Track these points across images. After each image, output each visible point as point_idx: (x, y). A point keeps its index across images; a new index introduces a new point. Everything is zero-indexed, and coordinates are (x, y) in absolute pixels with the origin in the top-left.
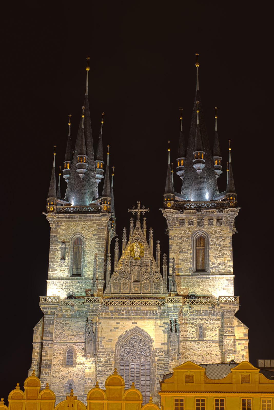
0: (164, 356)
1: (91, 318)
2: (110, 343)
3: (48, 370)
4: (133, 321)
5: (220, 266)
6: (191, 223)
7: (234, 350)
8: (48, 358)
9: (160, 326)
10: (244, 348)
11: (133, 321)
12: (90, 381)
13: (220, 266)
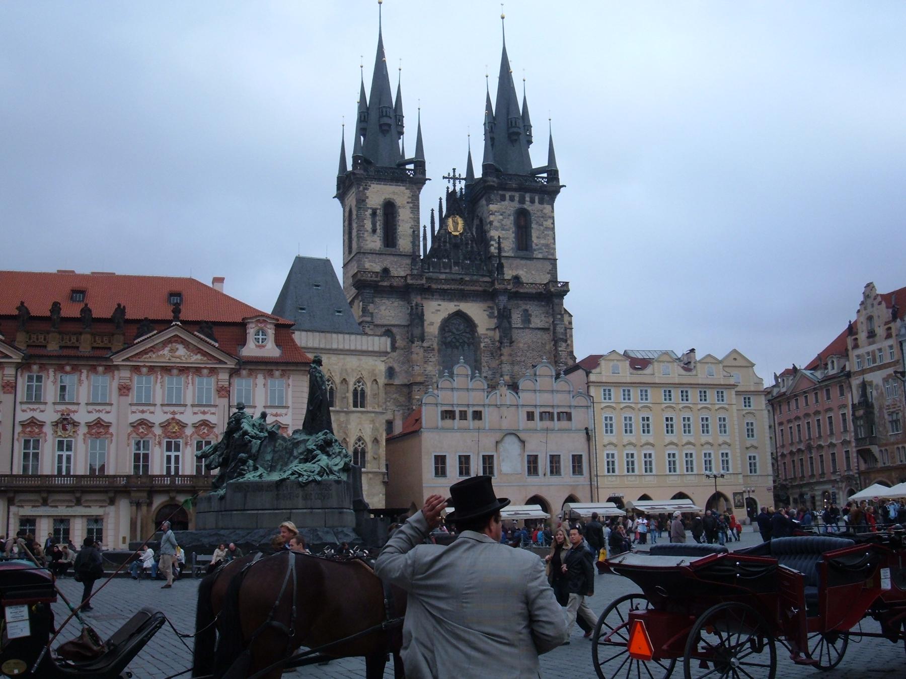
6: (512, 199)
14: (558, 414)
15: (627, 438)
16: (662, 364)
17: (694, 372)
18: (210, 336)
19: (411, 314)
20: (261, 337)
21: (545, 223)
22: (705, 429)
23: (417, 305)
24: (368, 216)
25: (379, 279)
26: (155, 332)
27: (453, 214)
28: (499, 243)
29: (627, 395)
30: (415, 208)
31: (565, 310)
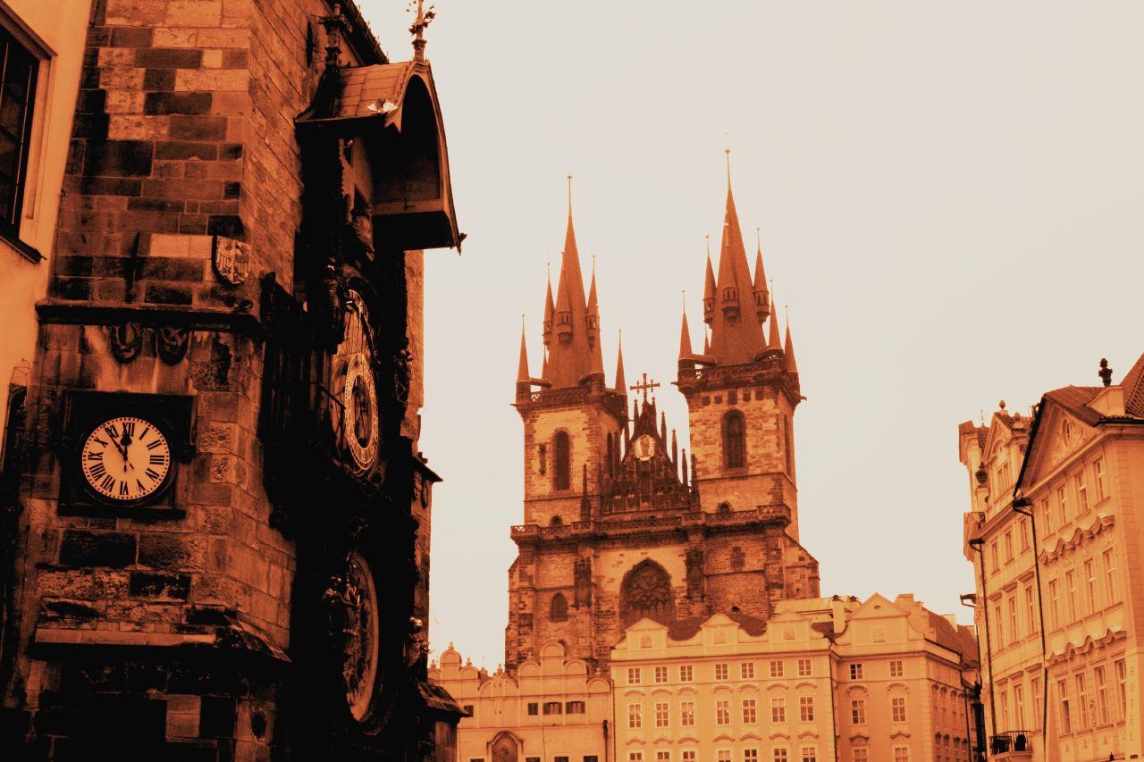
2: (612, 584)
3: (526, 628)
5: (763, 459)
6: (719, 400)
8: (528, 611)
9: (680, 556)
10: (798, 578)
11: (643, 551)
12: (582, 641)
14: (568, 704)
15: (660, 732)
16: (713, 629)
17: (763, 637)
19: (575, 574)
22: (778, 715)
23: (583, 561)
27: (642, 434)
29: (661, 675)
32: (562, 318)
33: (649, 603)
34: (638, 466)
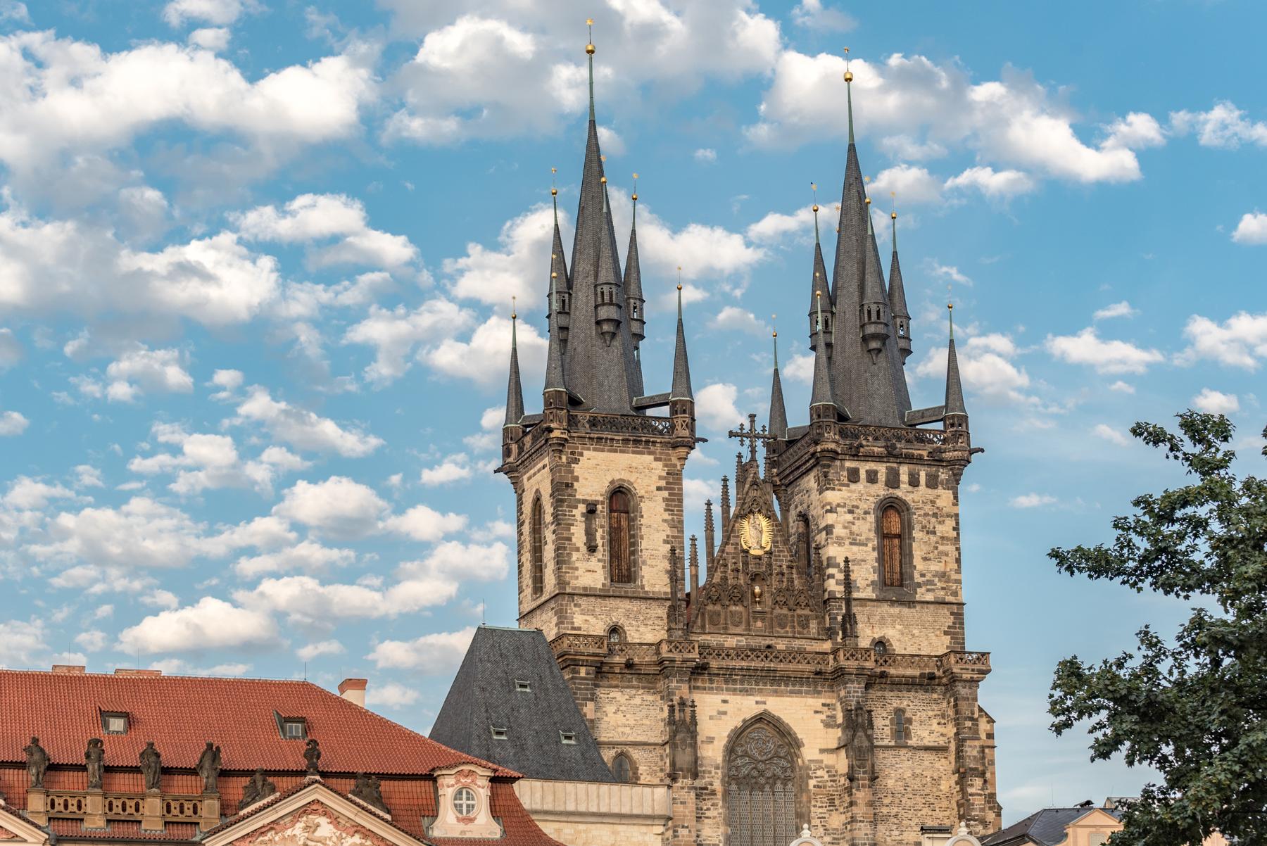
0: (826, 777)
1: (677, 688)
2: (710, 746)
4: (758, 699)
5: (936, 580)
6: (872, 478)
7: (981, 768)
9: (816, 712)
11: (758, 699)
12: (685, 832)
13: (936, 580)
18: (378, 800)
19: (671, 721)
20: (464, 802)
21: (939, 528)
23: (682, 703)
24: (579, 517)
25: (604, 650)
26: (278, 794)
27: (751, 512)
28: (847, 572)
30: (675, 501)
31: (981, 710)
32: (611, 294)
33: (762, 780)
34: (746, 564)
